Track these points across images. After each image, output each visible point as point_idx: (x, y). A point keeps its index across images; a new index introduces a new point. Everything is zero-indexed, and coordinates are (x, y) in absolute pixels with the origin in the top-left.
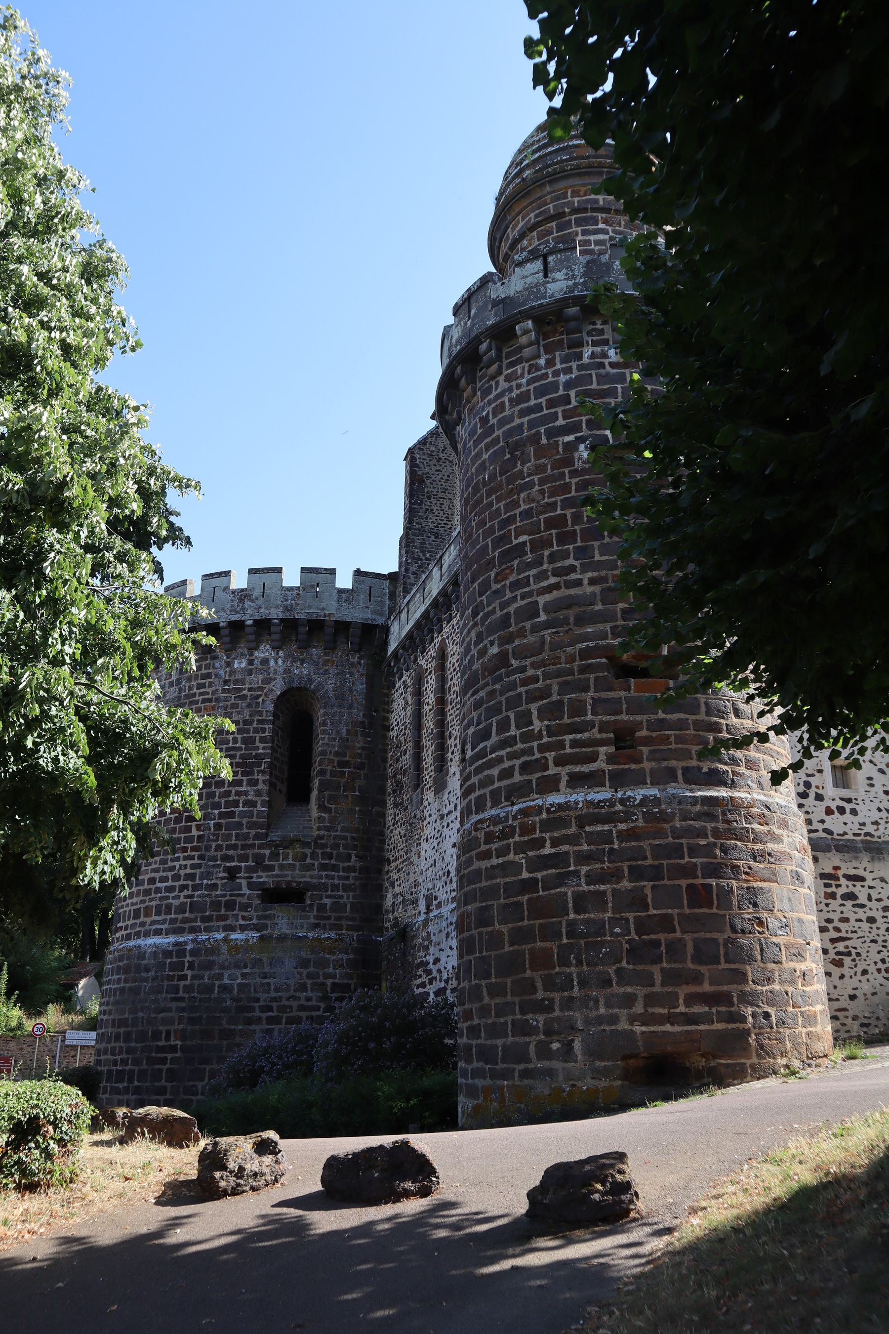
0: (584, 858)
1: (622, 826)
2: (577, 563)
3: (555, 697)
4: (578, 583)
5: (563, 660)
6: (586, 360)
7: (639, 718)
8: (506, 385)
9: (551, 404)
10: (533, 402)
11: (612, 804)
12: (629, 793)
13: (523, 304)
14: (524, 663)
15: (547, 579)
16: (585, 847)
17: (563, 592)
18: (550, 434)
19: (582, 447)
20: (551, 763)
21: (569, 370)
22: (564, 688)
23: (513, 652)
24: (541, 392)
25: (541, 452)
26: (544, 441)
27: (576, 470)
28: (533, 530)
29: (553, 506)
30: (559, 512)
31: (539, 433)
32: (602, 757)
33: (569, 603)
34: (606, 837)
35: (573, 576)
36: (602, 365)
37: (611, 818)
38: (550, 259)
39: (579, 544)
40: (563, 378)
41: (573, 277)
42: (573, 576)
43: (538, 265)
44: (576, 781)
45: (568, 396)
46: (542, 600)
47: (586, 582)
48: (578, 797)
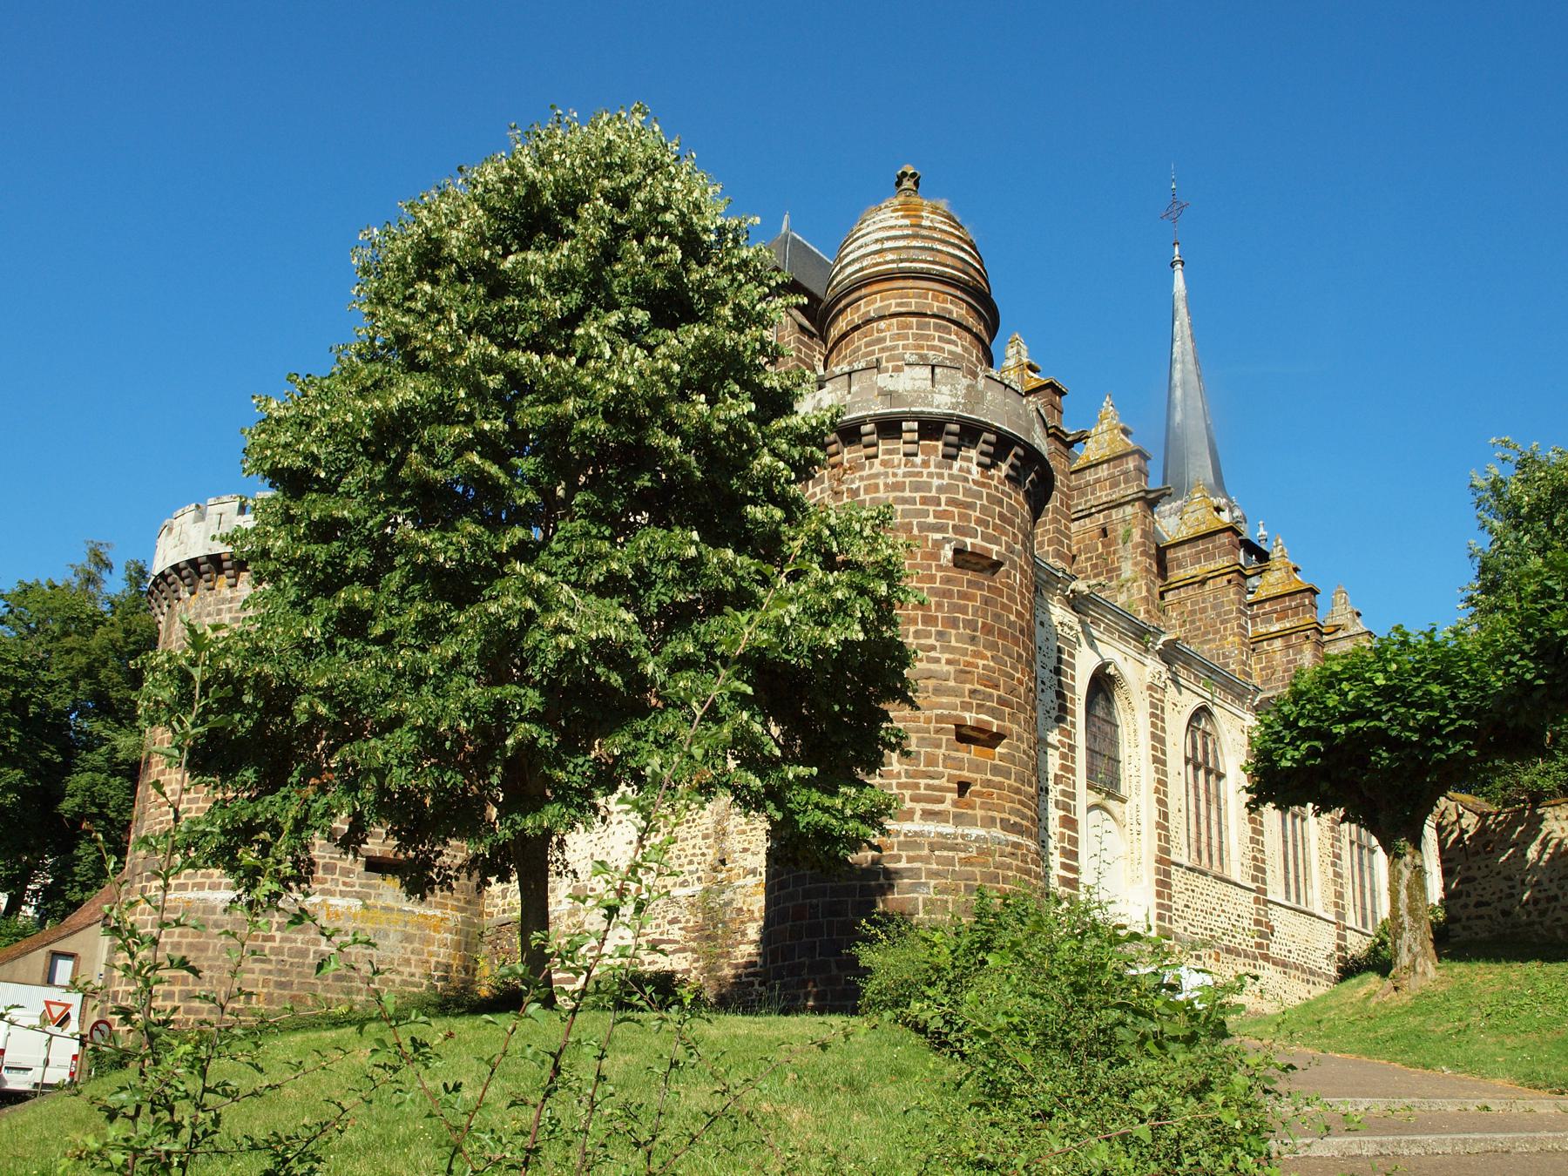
0: (933, 874)
1: (962, 855)
2: (938, 644)
4: (937, 660)
6: (955, 471)
7: (975, 776)
9: (924, 501)
10: (907, 494)
11: (956, 838)
12: (966, 831)
16: (934, 866)
18: (922, 527)
19: (947, 546)
21: (941, 476)
24: (917, 487)
26: (915, 531)
27: (941, 566)
31: (911, 523)
32: (948, 801)
34: (950, 861)
35: (933, 654)
36: (966, 480)
37: (953, 848)
38: (937, 370)
39: (940, 628)
40: (936, 482)
41: (956, 396)
42: (933, 654)
44: (928, 815)
45: (939, 499)
47: (943, 661)
48: (932, 828)
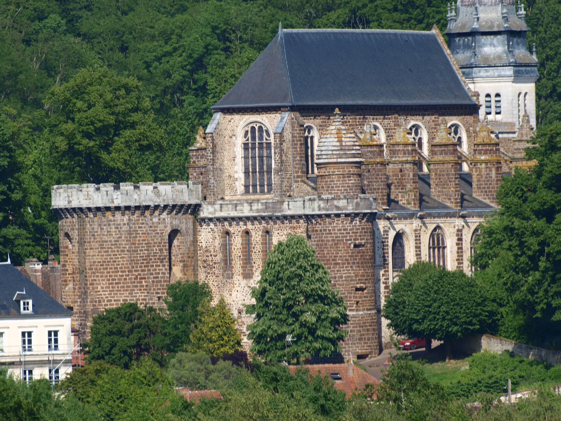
22: (348, 293)
24: (345, 230)
25: (344, 244)
28: (342, 260)
29: (346, 256)
33: (349, 277)
34: (355, 321)
37: (356, 317)
40: (349, 228)
43: (345, 201)
44: (350, 310)
46: (344, 275)
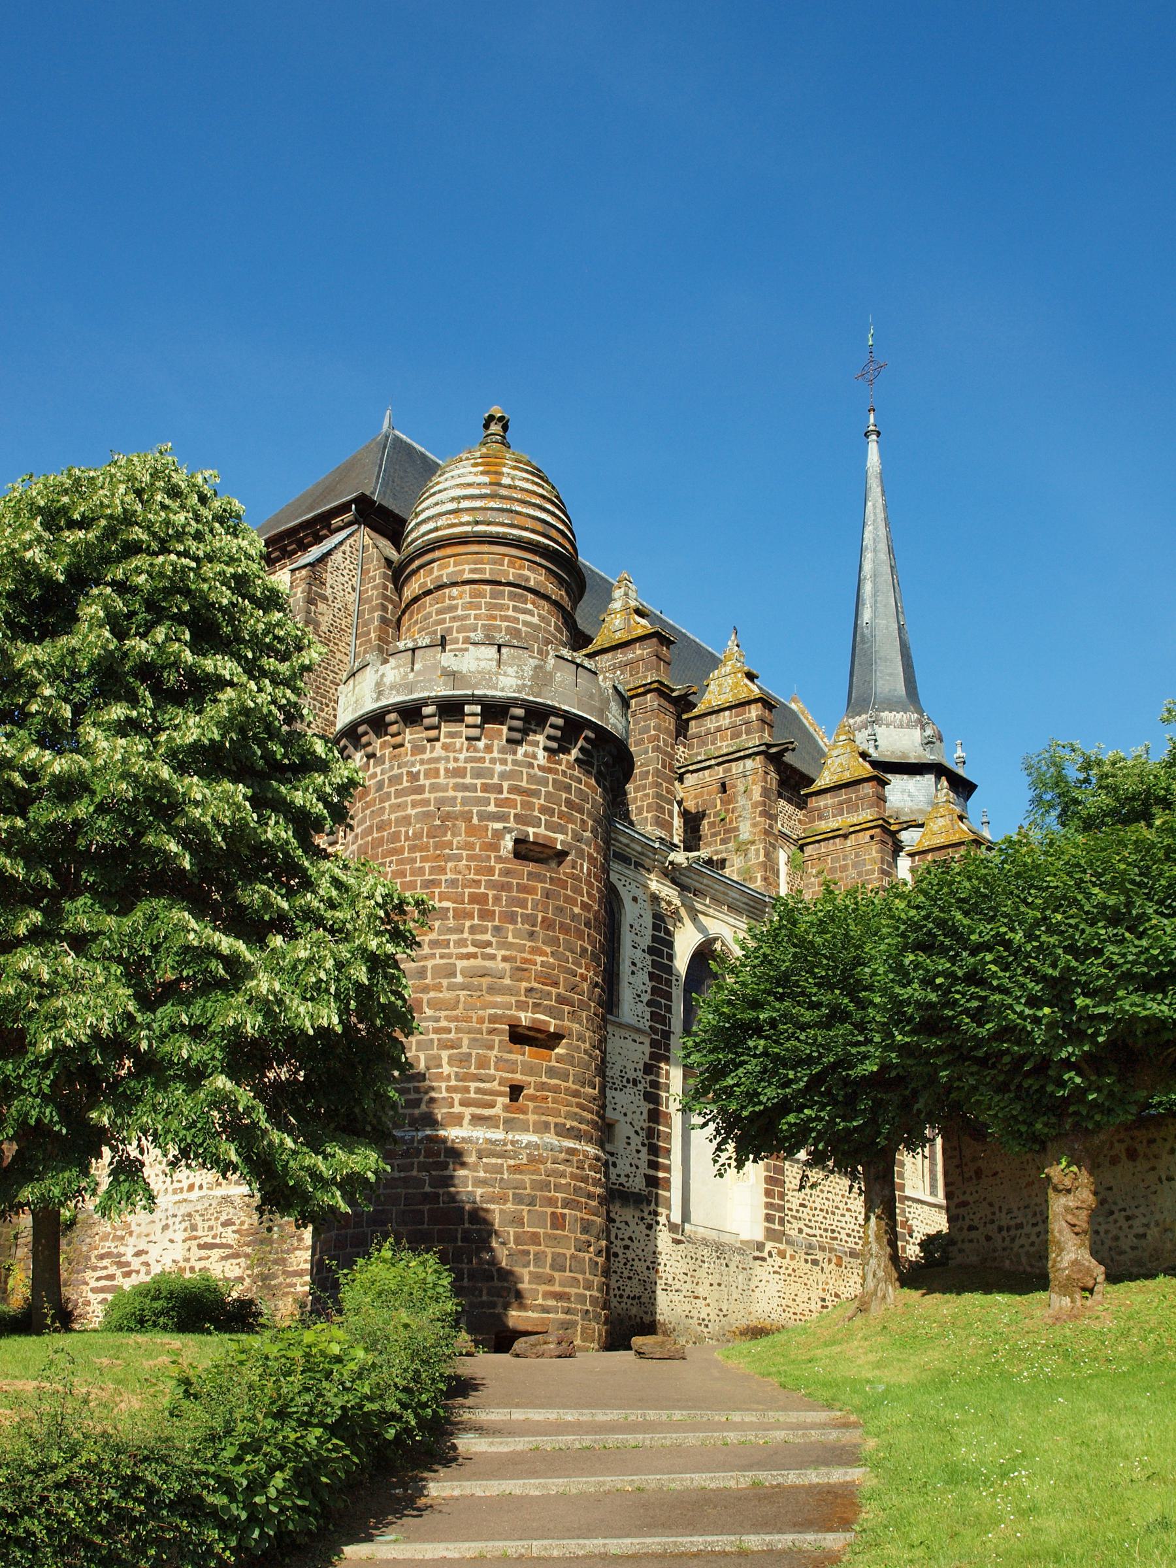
1: (512, 1162)
2: (494, 940)
3: (465, 1049)
4: (493, 957)
5: (474, 1020)
7: (529, 1079)
8: (443, 753)
11: (505, 1145)
12: (517, 1137)
13: (475, 687)
14: (437, 1014)
15: (467, 946)
16: (482, 1174)
17: (479, 962)
19: (508, 837)
20: (456, 1103)
21: (504, 762)
22: (474, 1042)
23: (428, 1003)
24: (478, 774)
25: (471, 830)
26: (475, 821)
27: (501, 857)
30: (482, 890)
32: (499, 1105)
34: (498, 1169)
38: (504, 650)
39: (497, 923)
40: (498, 768)
42: (488, 950)
44: (477, 1120)
